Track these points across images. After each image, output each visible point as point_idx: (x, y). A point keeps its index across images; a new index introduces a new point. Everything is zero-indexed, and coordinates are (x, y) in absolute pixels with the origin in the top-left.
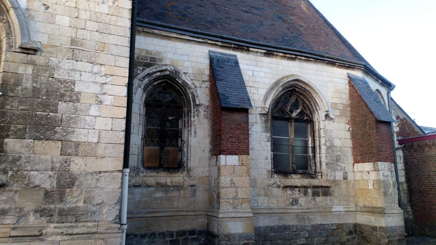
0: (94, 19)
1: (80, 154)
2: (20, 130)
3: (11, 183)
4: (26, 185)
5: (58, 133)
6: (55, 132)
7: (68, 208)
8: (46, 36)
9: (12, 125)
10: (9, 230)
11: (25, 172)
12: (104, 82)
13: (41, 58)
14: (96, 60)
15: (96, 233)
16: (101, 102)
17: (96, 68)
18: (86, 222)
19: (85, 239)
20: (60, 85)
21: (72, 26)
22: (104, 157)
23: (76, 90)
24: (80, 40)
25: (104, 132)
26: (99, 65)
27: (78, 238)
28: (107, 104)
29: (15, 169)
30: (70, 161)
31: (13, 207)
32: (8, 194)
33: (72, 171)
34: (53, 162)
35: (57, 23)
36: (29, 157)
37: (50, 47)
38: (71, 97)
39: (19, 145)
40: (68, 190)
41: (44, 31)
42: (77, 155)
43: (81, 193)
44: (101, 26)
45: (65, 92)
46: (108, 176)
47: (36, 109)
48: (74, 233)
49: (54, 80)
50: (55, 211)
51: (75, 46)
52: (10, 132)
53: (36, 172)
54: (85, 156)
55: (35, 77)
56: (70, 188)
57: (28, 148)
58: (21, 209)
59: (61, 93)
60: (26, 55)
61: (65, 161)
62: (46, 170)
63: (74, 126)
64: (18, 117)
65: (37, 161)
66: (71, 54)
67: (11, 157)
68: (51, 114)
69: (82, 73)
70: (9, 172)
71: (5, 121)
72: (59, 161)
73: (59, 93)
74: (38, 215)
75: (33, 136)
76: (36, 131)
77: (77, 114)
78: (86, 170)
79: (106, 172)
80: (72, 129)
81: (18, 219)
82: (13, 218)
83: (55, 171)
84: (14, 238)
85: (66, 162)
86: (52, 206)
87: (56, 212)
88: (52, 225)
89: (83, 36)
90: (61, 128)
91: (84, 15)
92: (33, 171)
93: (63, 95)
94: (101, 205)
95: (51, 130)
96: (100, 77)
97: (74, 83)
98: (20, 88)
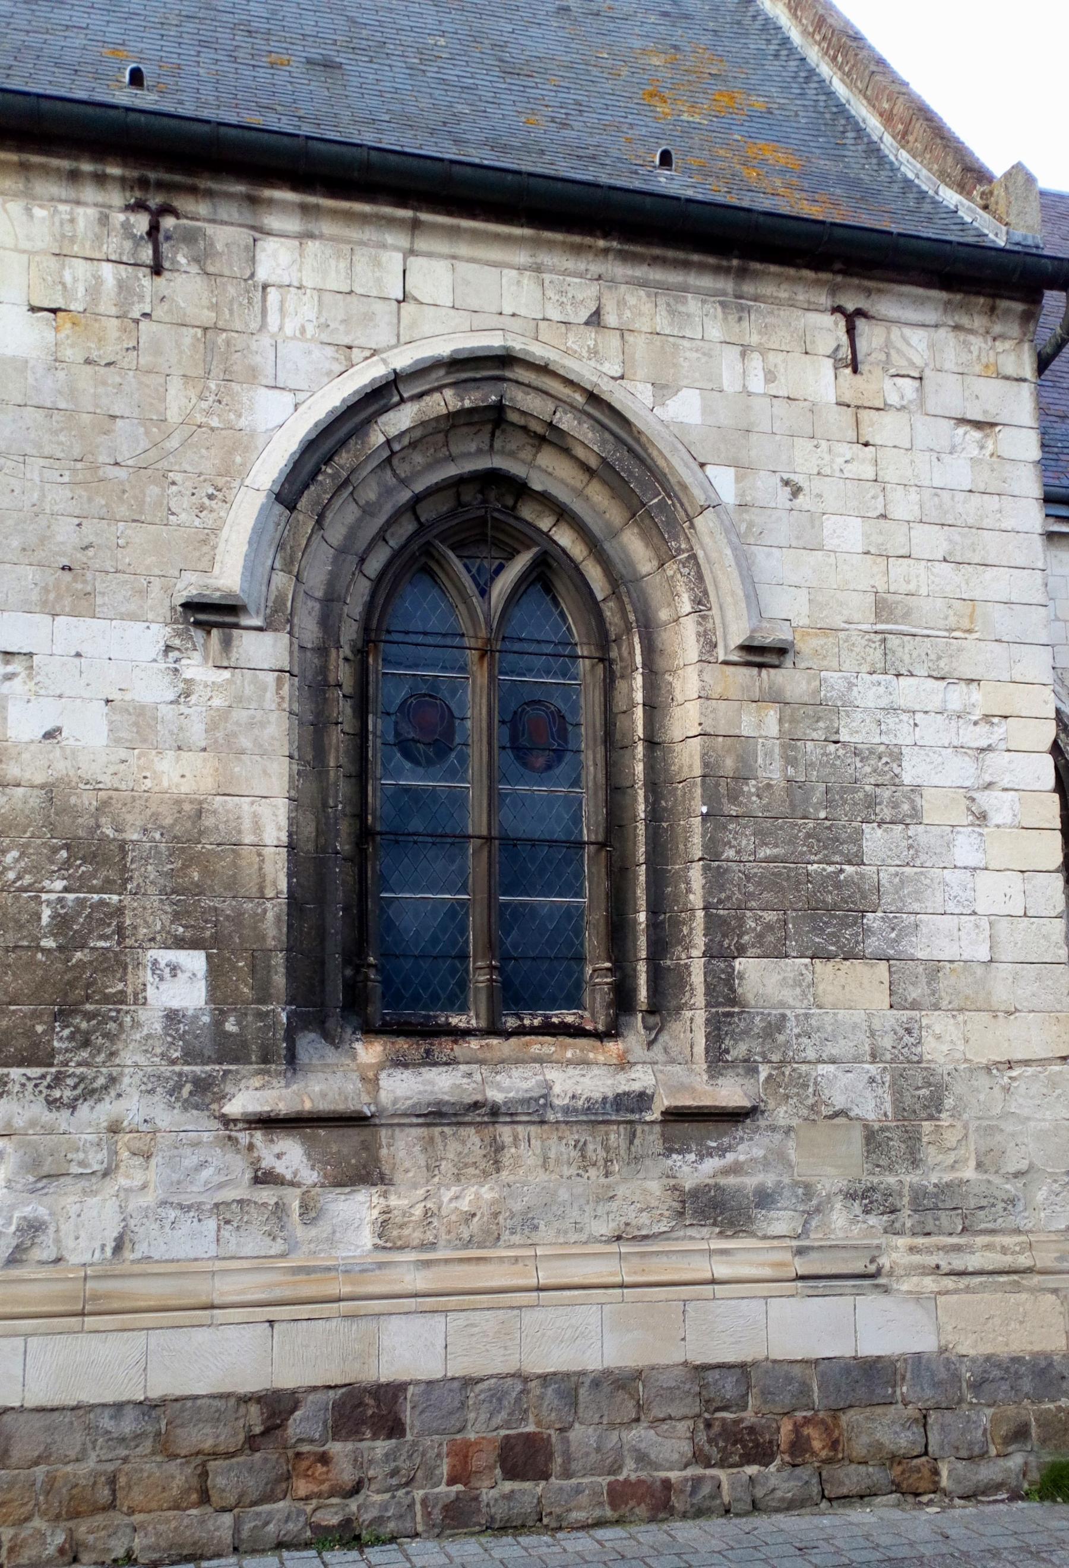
0: (934, 515)
1: (944, 1004)
2: (769, 927)
3: (772, 1103)
4: (812, 1108)
5: (874, 934)
6: (867, 931)
7: (936, 1185)
8: (803, 596)
9: (749, 914)
10: (788, 1256)
11: (804, 1068)
12: (984, 744)
13: (798, 675)
14: (954, 665)
15: (1029, 1270)
16: (982, 817)
17: (956, 697)
18: (992, 1232)
19: (1002, 1288)
20: (859, 765)
21: (873, 551)
22: (1017, 1010)
23: (907, 778)
24: (899, 598)
25: (1004, 923)
26: (963, 684)
27: (983, 1287)
28: (1000, 822)
29: (775, 1058)
30: (921, 1027)
31: (786, 1180)
32: (767, 1140)
33: (929, 1061)
34: (872, 1034)
35: (830, 543)
36: (807, 1016)
37: (816, 635)
38: (896, 806)
39: (776, 978)
40: (927, 1126)
41: (794, 579)
42: (936, 1007)
43: (966, 1136)
44: (957, 538)
45: (878, 790)
46: (1035, 1076)
47: (803, 854)
48: (970, 1269)
49: (841, 752)
50: (901, 1195)
51: (887, 623)
52: (746, 938)
53: (831, 1068)
54: (961, 1010)
55: (790, 743)
56: (931, 1118)
57: (800, 986)
58: (809, 1191)
59: (867, 795)
60: (755, 671)
61: (906, 1029)
62: (857, 1060)
63: (916, 907)
64: (759, 884)
65: (829, 1029)
66: (879, 653)
67: (758, 1018)
68: (849, 869)
69: (919, 717)
70: (761, 1067)
71: (729, 898)
72: (889, 1029)
73: (861, 795)
74: (857, 1207)
75: (807, 949)
76: (814, 929)
77: (918, 864)
78: (969, 1057)
79: (1027, 1063)
80: (912, 917)
81: (806, 1222)
82: (792, 1218)
83: (881, 1061)
84: (811, 1283)
85: (909, 1031)
86: (891, 1180)
87: (906, 1200)
88: (902, 1242)
89: (908, 582)
90: (880, 914)
91: (903, 506)
92: (824, 1062)
93: (872, 802)
94: (1029, 1176)
95: (855, 924)
96: (971, 727)
97: (896, 756)
98: (751, 787)
